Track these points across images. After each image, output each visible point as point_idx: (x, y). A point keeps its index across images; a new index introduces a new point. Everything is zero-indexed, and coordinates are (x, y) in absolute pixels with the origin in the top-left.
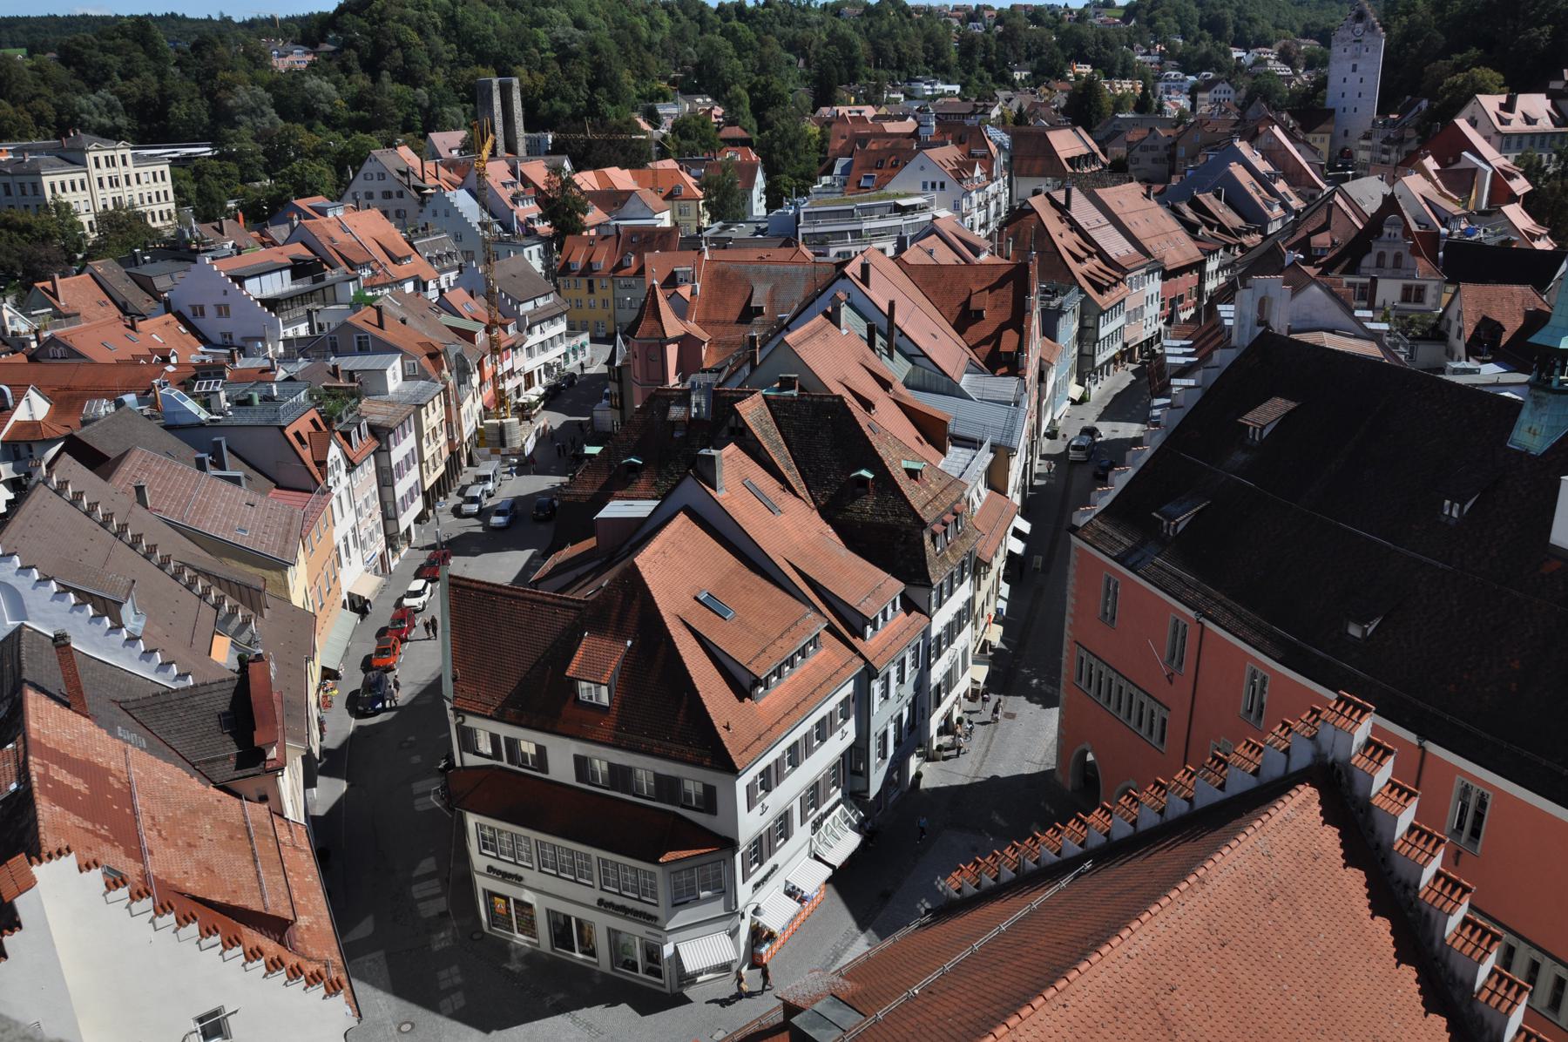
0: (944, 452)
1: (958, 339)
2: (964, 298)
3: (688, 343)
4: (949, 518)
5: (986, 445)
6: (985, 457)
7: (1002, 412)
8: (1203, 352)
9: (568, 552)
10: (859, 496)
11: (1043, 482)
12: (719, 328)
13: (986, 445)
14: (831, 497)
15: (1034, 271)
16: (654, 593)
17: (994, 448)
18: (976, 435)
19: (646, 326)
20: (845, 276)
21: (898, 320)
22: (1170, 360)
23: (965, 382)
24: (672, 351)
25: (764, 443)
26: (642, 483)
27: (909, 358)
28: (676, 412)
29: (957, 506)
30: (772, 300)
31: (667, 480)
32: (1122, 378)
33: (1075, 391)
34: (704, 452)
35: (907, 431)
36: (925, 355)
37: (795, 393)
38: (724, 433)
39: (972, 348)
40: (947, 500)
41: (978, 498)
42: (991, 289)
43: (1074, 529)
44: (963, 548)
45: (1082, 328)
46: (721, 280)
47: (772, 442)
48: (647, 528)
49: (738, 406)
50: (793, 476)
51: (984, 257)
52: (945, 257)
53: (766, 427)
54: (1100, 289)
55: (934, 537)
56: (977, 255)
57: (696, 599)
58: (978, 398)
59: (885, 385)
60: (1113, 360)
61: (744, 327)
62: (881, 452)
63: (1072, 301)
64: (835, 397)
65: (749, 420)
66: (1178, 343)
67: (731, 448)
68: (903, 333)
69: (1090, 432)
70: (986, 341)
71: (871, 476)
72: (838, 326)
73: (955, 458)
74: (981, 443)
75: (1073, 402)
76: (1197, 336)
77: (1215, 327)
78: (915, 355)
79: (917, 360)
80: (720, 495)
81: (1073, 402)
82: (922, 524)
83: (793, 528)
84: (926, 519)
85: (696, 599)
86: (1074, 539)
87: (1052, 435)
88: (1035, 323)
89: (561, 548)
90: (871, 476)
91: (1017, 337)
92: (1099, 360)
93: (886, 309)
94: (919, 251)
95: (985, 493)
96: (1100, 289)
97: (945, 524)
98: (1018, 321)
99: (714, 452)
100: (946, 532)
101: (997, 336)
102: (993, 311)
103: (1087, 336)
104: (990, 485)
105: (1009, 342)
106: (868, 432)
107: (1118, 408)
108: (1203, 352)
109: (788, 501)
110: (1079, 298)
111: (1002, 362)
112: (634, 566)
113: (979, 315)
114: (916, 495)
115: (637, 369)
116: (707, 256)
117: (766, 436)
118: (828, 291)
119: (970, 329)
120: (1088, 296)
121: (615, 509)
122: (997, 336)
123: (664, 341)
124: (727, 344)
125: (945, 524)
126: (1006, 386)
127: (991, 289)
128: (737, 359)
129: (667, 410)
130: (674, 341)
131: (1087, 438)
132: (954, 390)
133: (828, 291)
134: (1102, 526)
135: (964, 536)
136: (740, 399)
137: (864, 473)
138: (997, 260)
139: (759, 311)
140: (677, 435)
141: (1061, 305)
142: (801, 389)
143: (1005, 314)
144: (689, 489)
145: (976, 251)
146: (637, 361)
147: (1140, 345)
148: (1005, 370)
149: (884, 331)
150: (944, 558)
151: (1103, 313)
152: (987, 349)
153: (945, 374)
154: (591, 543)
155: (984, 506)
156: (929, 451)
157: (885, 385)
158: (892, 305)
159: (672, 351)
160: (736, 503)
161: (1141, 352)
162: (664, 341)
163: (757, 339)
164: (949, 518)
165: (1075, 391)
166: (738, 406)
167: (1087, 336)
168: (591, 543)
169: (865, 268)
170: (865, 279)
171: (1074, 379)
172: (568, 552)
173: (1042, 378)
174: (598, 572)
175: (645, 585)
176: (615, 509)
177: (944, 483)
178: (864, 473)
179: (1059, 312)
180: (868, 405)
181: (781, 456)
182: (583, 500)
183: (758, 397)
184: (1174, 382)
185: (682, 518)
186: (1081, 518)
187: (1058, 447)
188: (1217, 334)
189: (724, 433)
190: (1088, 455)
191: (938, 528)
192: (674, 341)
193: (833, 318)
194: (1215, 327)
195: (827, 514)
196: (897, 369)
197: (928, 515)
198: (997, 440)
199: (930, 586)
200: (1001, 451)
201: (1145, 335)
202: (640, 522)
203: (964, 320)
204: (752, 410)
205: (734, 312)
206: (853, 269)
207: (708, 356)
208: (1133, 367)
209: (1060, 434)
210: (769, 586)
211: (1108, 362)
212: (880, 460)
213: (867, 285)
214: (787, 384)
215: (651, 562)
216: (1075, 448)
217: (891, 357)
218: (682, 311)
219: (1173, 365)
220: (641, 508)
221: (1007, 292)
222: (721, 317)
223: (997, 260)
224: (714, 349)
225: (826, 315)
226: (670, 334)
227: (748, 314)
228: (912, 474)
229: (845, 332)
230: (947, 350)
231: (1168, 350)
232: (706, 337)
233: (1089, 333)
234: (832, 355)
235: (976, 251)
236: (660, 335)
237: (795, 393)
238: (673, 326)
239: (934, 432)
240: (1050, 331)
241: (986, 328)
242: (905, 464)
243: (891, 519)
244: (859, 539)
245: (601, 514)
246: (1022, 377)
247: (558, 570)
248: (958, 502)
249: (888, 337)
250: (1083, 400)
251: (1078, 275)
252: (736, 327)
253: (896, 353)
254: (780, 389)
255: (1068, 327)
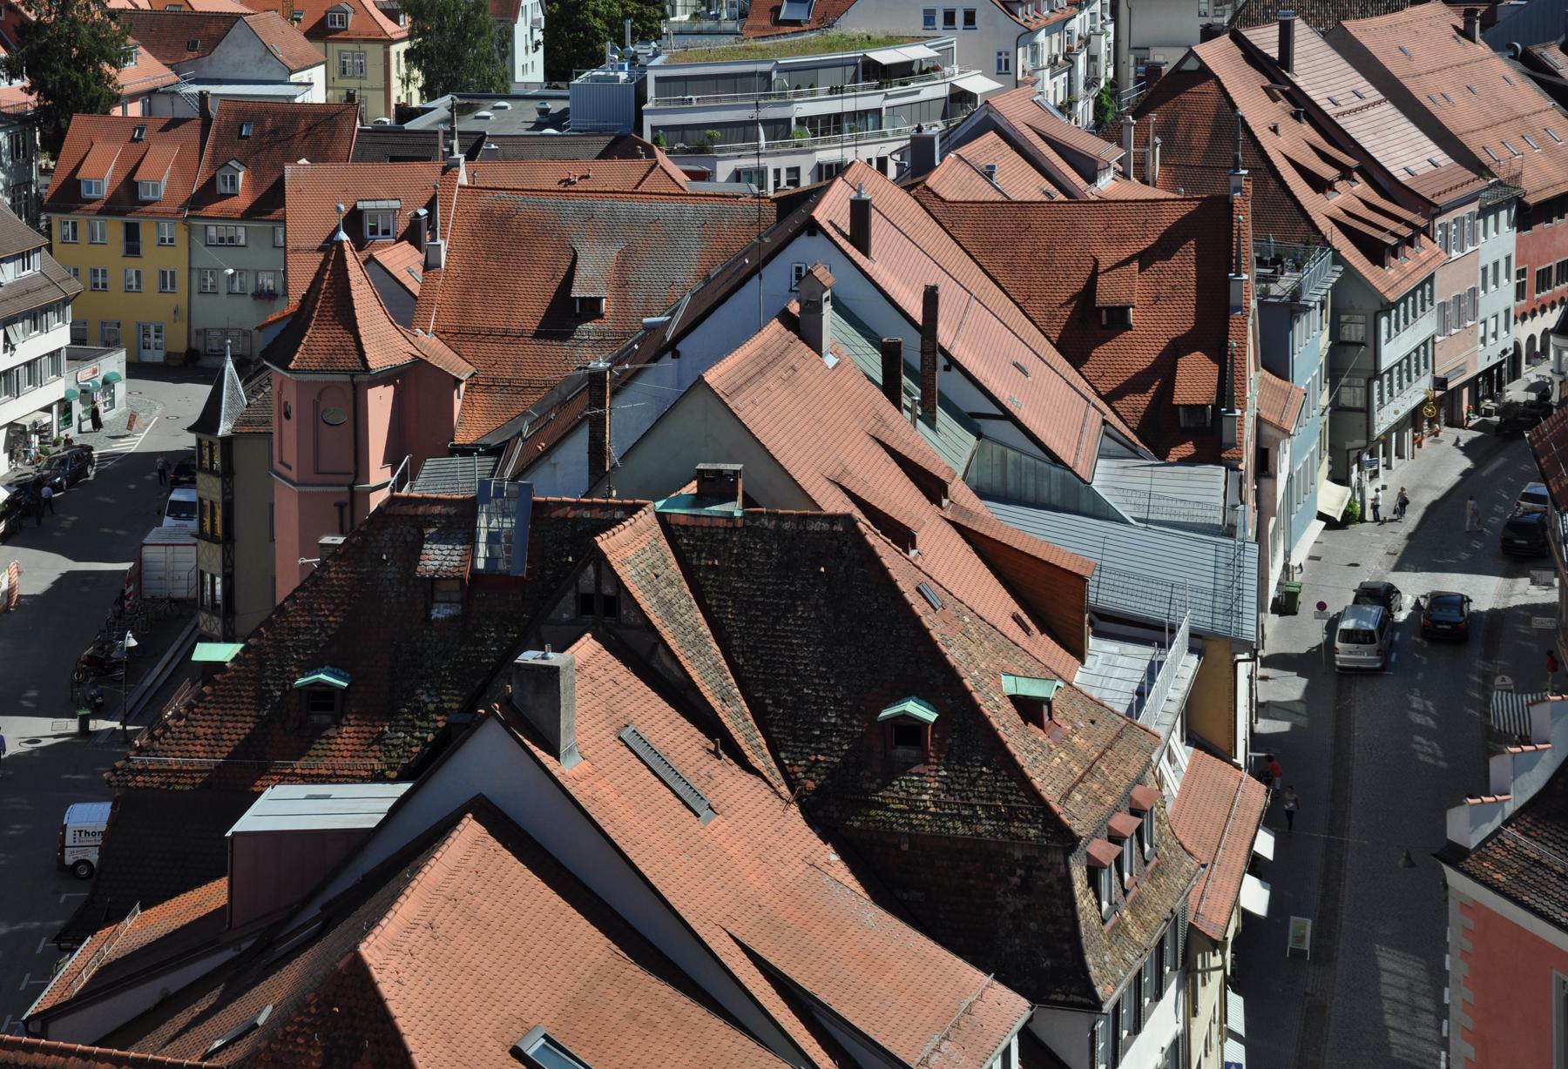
0: (1079, 653)
1: (1071, 374)
2: (1078, 282)
3: (418, 385)
4: (1125, 823)
5: (1182, 636)
6: (1181, 667)
7: (1204, 551)
9: (140, 927)
10: (905, 768)
11: (1283, 726)
12: (496, 349)
13: (1182, 636)
14: (832, 771)
15: (1243, 216)
16: (410, 1042)
17: (1200, 642)
18: (1152, 609)
19: (317, 341)
20: (813, 228)
21: (944, 336)
23: (1106, 478)
24: (380, 402)
25: (667, 633)
26: (347, 736)
27: (969, 421)
28: (437, 558)
29: (1138, 793)
30: (622, 284)
31: (410, 728)
32: (1439, 464)
33: (1332, 498)
34: (529, 657)
35: (997, 603)
36: (1008, 416)
37: (735, 508)
38: (566, 610)
39: (1108, 398)
40: (1117, 776)
41: (1157, 772)
42: (1145, 259)
43: (1456, 855)
44: (1162, 904)
45: (1339, 346)
46: (499, 232)
47: (685, 630)
48: (371, 860)
49: (604, 542)
50: (736, 716)
51: (1106, 184)
52: (1024, 184)
53: (669, 593)
54: (1377, 253)
55: (1094, 872)
56: (1091, 179)
57: (517, 1053)
58: (1144, 521)
59: (932, 487)
60: (1414, 418)
61: (554, 349)
62: (954, 655)
63: (1318, 281)
64: (833, 518)
65: (629, 576)
67: (586, 648)
68: (952, 363)
69: (1379, 595)
70: (1135, 384)
71: (930, 716)
72: (817, 347)
73: (1109, 668)
74: (1173, 631)
75: (1331, 524)
78: (985, 416)
79: (989, 427)
80: (567, 769)
81: (1331, 524)
82: (1067, 840)
83: (743, 854)
84: (1076, 827)
85: (517, 1053)
86: (1453, 877)
87: (1286, 605)
88: (1247, 339)
89: (115, 915)
90: (930, 716)
91: (1210, 370)
92: (1384, 419)
93: (917, 313)
94: (963, 171)
95: (1184, 753)
96: (1377, 253)
97: (1116, 839)
98: (1210, 331)
99: (554, 659)
100: (1119, 861)
101: (1164, 370)
102: (1155, 310)
103: (1350, 362)
104: (1193, 738)
105: (1194, 381)
106: (919, 607)
107: (1438, 537)
109: (727, 780)
110: (1333, 275)
111: (1175, 428)
112: (359, 969)
113: (1118, 319)
114: (1045, 763)
115: (289, 442)
116: (463, 179)
117: (670, 616)
118: (777, 255)
119: (1101, 354)
120: (1350, 272)
121: (280, 809)
122: (1164, 370)
123: (362, 378)
124: (514, 388)
125: (1116, 839)
126: (1199, 488)
127: (1145, 259)
128: (541, 424)
129: (415, 553)
130: (385, 378)
131: (1375, 611)
132: (1077, 499)
133: (777, 255)
134: (1532, 848)
135: (1160, 870)
136: (608, 525)
137: (913, 708)
138: (1134, 190)
139: (591, 308)
140: (440, 612)
141: (1296, 294)
142: (748, 501)
143: (1180, 317)
144: (488, 756)
145: (1089, 169)
146: (290, 427)
147: (1472, 383)
148: (1188, 449)
149: (914, 367)
150: (1120, 930)
151: (1387, 308)
152: (1143, 401)
153: (1055, 460)
154: (212, 895)
155: (1186, 789)
156: (1045, 647)
157: (932, 487)
158: (931, 298)
159: (380, 402)
160: (605, 791)
161: (1475, 401)
162: (362, 378)
163: (606, 376)
164: (1125, 823)
165: (1332, 498)
166: (604, 542)
167: (1350, 362)
168: (212, 895)
169: (860, 210)
170: (860, 236)
171: (1325, 468)
172: (140, 927)
173: (1264, 466)
174: (237, 980)
175: (387, 1019)
176: (280, 809)
177: (1105, 732)
178: (913, 708)
179: (1293, 308)
180: (903, 537)
181: (706, 667)
182: (184, 785)
183: (645, 519)
185: (470, 830)
186: (1466, 825)
187: (1306, 633)
189: (566, 610)
190: (1384, 653)
191: (1102, 850)
192: (385, 378)
193: (805, 329)
195: (825, 813)
196: (948, 447)
197: (1079, 816)
198: (1205, 621)
199: (1095, 1005)
200: (1216, 650)
201: (1484, 358)
202: (355, 840)
203: (1083, 330)
204: (634, 551)
205: (531, 309)
206: (832, 209)
207: (469, 419)
208: (1466, 436)
209: (1307, 605)
210: (697, 1013)
211: (1399, 427)
212: (951, 677)
213: (865, 249)
214: (716, 487)
215: (392, 950)
216: (1349, 636)
217: (931, 422)
218: (402, 306)
220: (360, 805)
221: (1184, 264)
222: (497, 321)
223: (1134, 190)
224: (480, 398)
225: (788, 321)
226: (377, 360)
227: (566, 314)
228: (1031, 710)
229: (830, 361)
230: (1056, 405)
232: (462, 369)
233: (1359, 358)
234: (813, 420)
235: (1089, 169)
236: (352, 363)
237: (735, 508)
238: (384, 344)
239: (1055, 604)
240: (1277, 361)
241: (1134, 352)
242: (1009, 685)
243: (985, 827)
244: (899, 877)
245: (248, 822)
246: (1232, 467)
247: (110, 980)
248: (1139, 781)
249: (925, 379)
250: (1351, 517)
251: (1325, 226)
252: (535, 347)
253: (941, 415)
254: (699, 500)
255: (1311, 342)
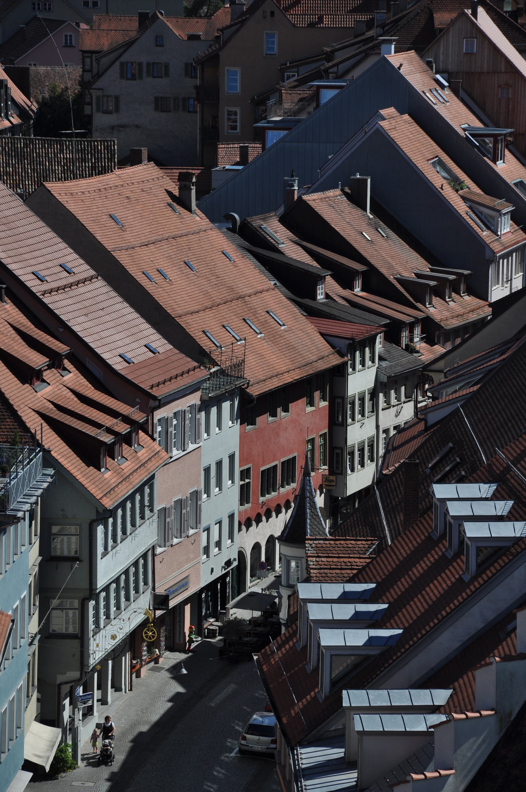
8: (417, 607)
22: (329, 638)
54: (92, 453)
66: (334, 590)
76: (388, 564)
77: (430, 543)
96: (92, 453)
108: (417, 607)
110: (43, 480)
120: (62, 475)
151: (104, 515)
184: (353, 698)
188: (443, 564)
194: (430, 543)
219: (339, 652)
231: (316, 612)
251: (33, 422)
